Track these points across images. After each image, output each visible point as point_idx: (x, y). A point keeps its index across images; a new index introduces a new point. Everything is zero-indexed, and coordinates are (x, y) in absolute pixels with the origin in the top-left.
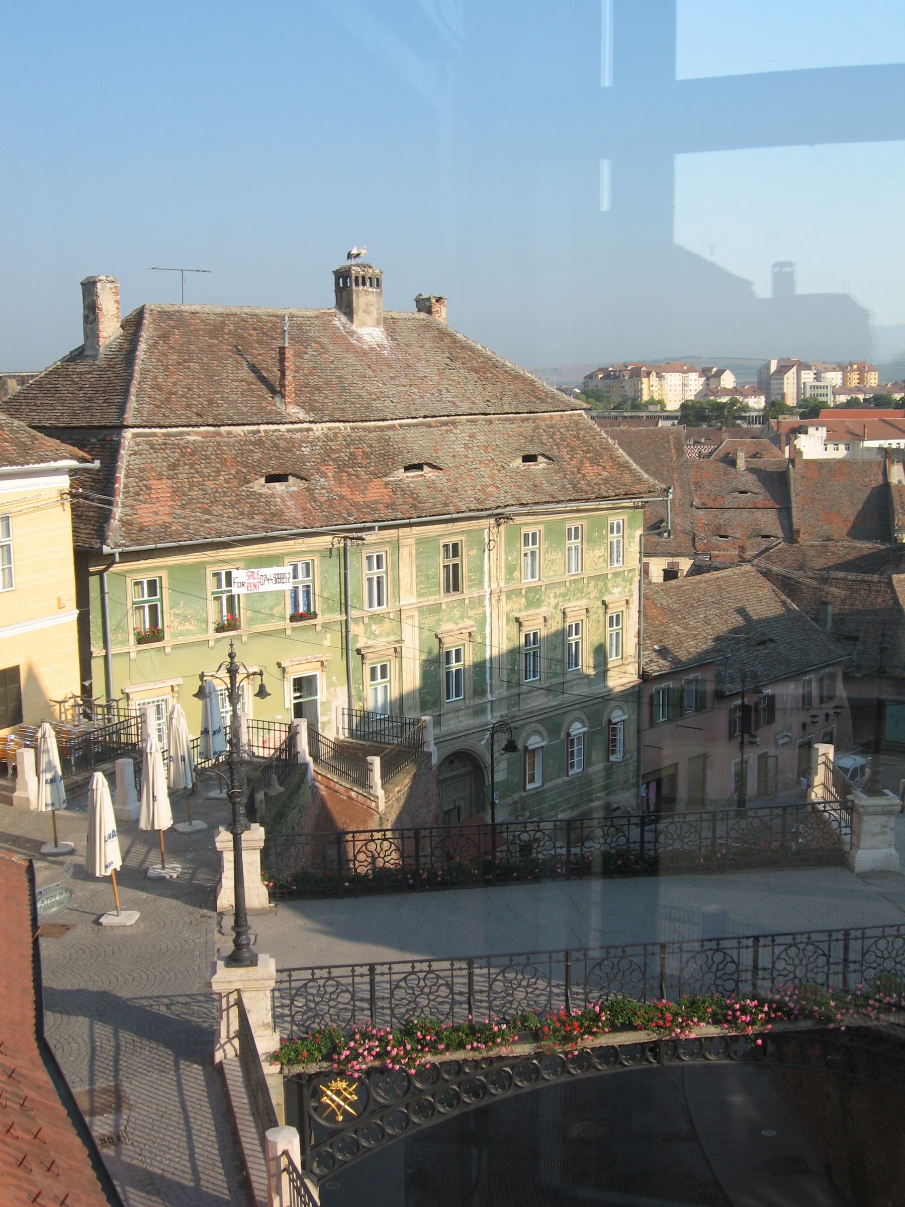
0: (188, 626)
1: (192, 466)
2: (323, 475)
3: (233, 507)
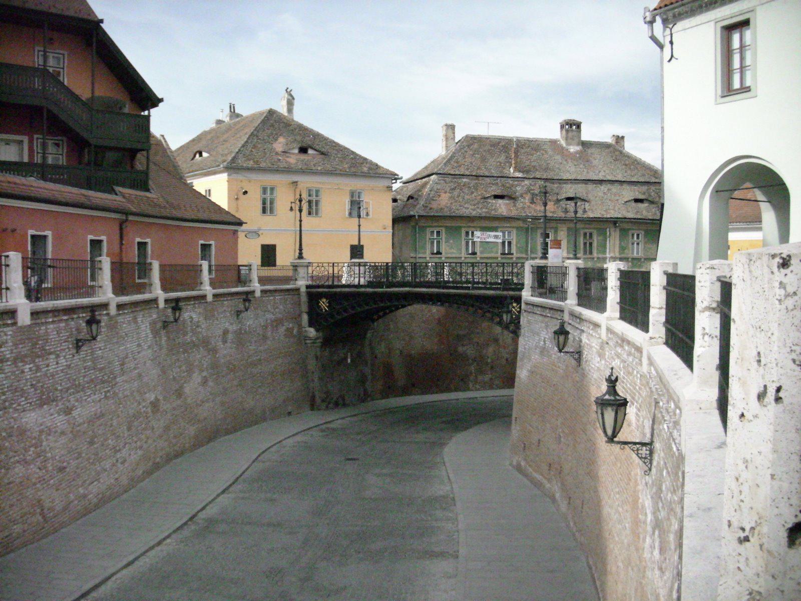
0: (453, 250)
1: (461, 190)
2: (525, 198)
3: (474, 205)
